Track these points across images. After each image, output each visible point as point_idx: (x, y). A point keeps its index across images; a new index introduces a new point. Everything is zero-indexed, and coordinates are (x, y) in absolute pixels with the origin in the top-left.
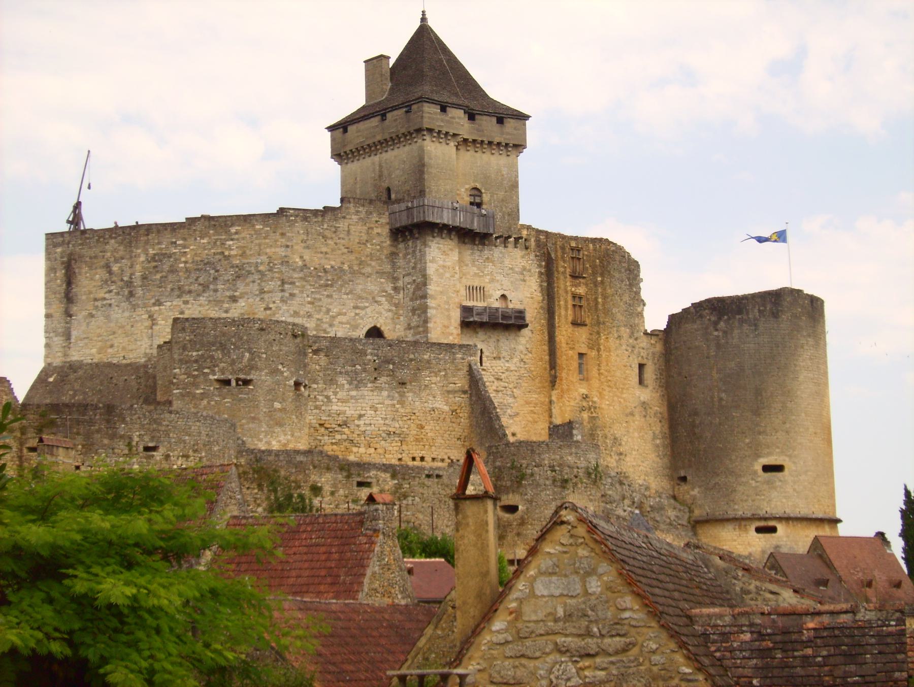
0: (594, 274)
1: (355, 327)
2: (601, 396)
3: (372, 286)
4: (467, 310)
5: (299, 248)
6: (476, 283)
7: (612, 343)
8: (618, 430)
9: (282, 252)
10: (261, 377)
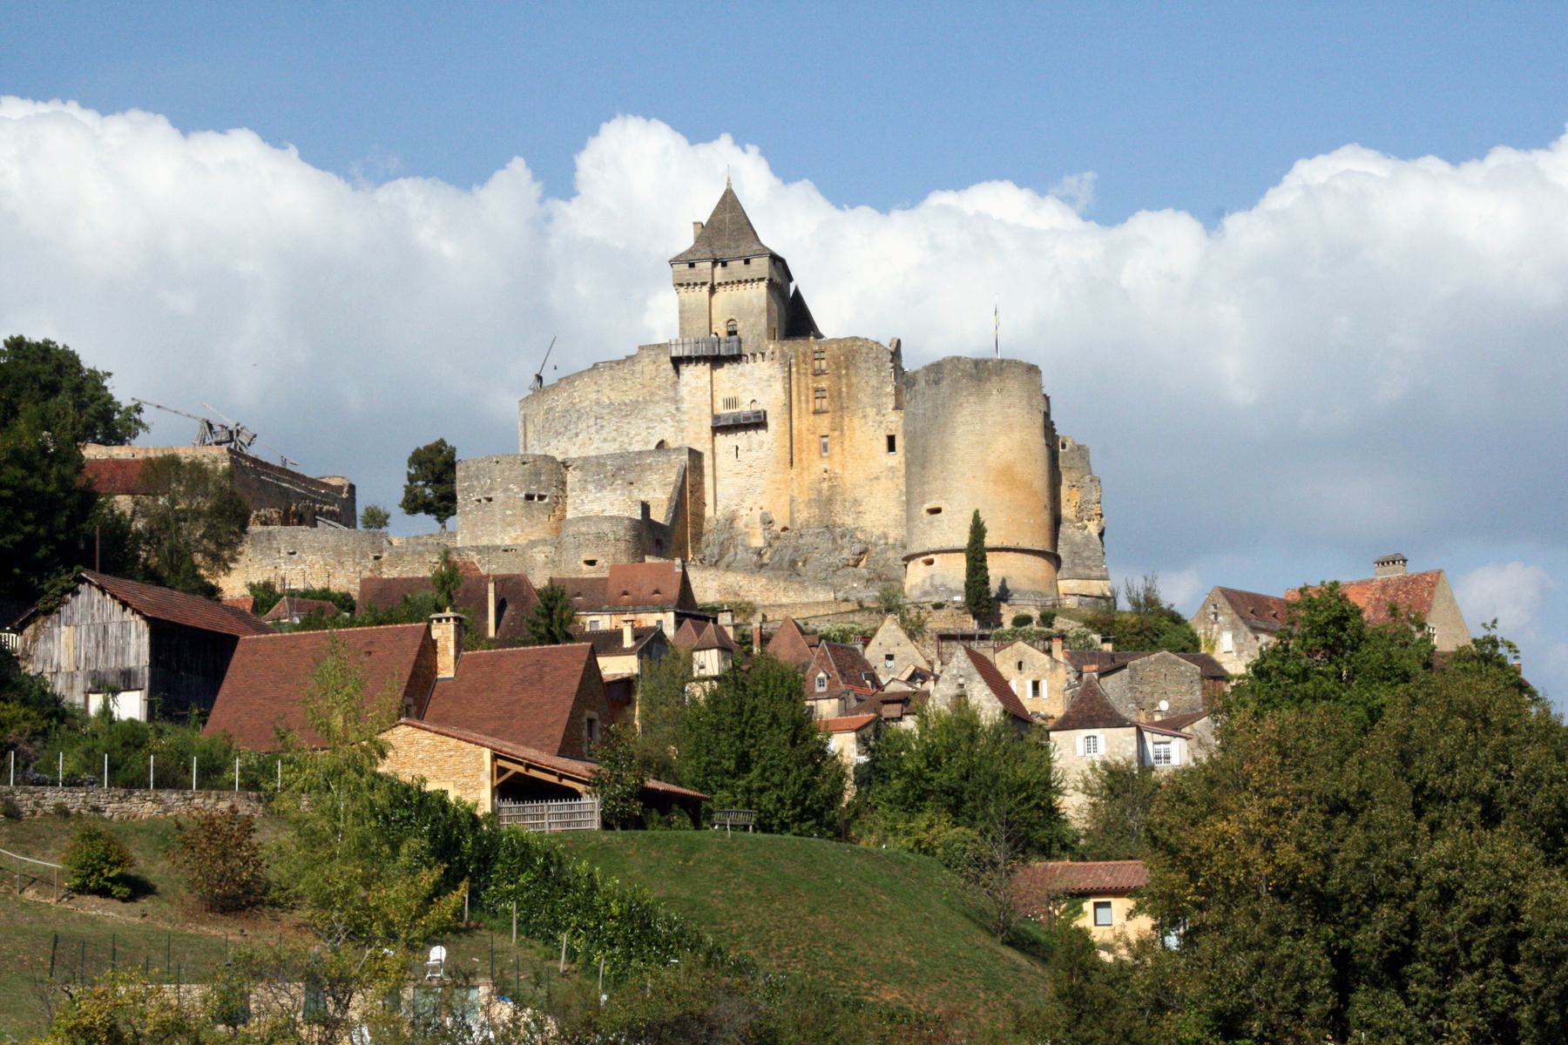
0: (838, 368)
1: (647, 443)
2: (843, 467)
3: (660, 410)
4: (716, 418)
5: (607, 391)
6: (731, 395)
7: (857, 422)
8: (859, 494)
9: (593, 396)
10: (498, 495)
